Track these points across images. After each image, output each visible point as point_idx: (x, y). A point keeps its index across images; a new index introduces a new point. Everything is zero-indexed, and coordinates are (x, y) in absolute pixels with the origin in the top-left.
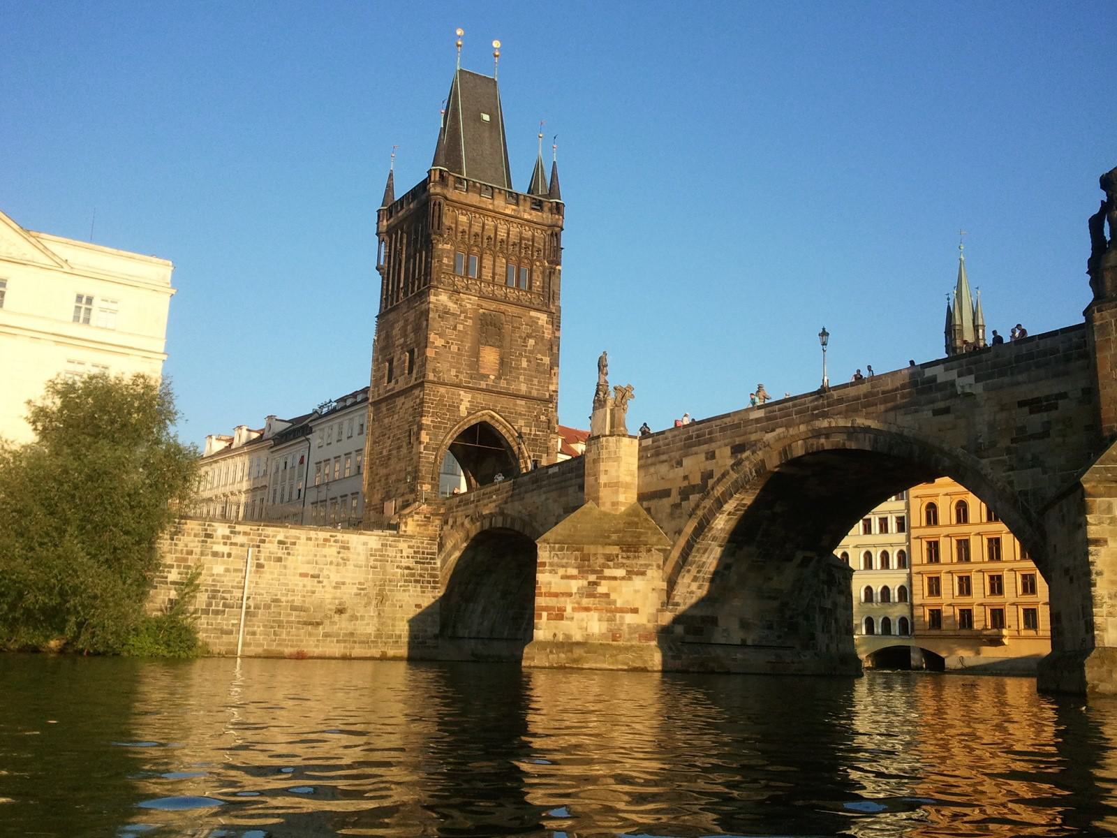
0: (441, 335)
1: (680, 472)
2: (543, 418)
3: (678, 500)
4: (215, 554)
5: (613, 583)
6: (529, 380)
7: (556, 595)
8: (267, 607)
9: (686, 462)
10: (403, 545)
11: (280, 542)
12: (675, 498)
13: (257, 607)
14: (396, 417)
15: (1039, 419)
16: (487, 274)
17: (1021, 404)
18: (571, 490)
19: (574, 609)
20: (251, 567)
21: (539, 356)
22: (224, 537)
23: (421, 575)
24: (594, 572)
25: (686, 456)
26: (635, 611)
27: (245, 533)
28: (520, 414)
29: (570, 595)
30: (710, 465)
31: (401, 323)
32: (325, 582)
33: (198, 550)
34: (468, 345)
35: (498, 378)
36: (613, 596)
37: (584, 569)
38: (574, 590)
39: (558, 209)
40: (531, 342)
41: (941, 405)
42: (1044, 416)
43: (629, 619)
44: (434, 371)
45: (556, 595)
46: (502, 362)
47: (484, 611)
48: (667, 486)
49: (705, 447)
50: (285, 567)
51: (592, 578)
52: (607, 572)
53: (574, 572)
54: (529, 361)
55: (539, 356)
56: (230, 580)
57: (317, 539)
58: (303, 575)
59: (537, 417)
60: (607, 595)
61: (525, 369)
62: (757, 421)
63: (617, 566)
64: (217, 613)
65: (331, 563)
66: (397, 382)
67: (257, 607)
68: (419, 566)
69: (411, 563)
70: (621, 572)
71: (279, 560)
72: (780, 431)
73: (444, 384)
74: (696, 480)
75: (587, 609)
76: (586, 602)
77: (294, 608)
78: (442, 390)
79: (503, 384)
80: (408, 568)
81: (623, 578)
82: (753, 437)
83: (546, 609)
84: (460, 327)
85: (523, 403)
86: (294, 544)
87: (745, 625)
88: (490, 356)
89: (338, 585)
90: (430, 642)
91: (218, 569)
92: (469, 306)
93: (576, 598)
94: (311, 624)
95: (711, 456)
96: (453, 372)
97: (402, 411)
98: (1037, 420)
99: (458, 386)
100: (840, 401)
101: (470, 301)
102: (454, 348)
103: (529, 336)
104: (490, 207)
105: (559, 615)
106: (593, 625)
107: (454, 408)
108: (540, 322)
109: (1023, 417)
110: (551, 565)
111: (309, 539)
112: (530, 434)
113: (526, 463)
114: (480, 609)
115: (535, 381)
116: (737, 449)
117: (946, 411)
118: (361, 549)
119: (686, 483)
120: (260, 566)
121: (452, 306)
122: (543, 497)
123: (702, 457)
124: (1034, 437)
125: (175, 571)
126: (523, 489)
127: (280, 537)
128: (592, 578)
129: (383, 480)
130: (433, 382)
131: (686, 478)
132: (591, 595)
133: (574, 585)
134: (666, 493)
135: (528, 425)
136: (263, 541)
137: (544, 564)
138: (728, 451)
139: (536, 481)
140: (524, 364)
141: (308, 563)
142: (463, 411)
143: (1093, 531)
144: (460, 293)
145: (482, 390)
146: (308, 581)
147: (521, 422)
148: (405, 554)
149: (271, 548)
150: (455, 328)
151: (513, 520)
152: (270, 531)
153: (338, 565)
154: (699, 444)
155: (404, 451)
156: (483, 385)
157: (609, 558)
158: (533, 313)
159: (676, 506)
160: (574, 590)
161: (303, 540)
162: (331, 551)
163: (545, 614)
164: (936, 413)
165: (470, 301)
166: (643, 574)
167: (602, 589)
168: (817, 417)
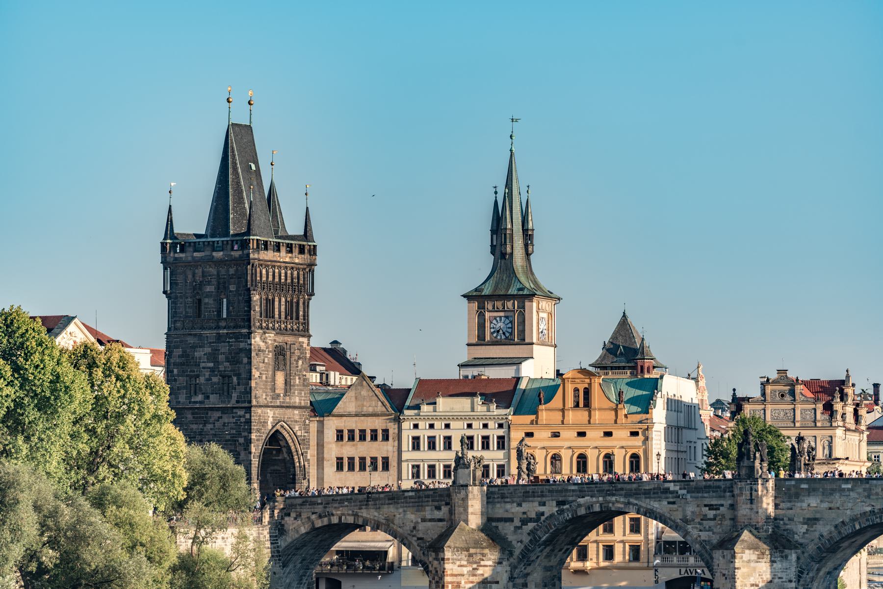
1: (521, 510)
3: (519, 524)
7: (456, 575)
9: (524, 504)
14: (209, 426)
15: (713, 512)
17: (706, 506)
21: (304, 373)
24: (476, 563)
25: (524, 501)
26: (497, 582)
28: (296, 421)
30: (542, 509)
31: (208, 350)
35: (285, 395)
38: (465, 573)
39: (313, 251)
40: (300, 362)
41: (671, 500)
42: (714, 512)
44: (256, 397)
45: (456, 575)
46: (287, 383)
47: (289, 573)
48: (510, 516)
51: (475, 566)
52: (482, 563)
53: (465, 563)
59: (304, 421)
62: (573, 491)
66: (208, 397)
72: (587, 498)
73: (261, 406)
74: (533, 515)
82: (571, 499)
83: (451, 583)
84: (266, 361)
88: (280, 377)
92: (270, 342)
93: (466, 577)
97: (218, 424)
98: (711, 514)
100: (622, 489)
102: (264, 376)
103: (299, 358)
109: (705, 510)
116: (560, 503)
117: (674, 503)
123: (536, 504)
124: (710, 519)
128: (475, 566)
130: (256, 406)
131: (524, 513)
133: (465, 570)
134: (511, 520)
137: (448, 559)
138: (554, 503)
139: (393, 499)
140: (297, 381)
143: (737, 565)
145: (278, 407)
154: (534, 497)
160: (465, 573)
163: (450, 586)
164: (669, 503)
168: (609, 495)
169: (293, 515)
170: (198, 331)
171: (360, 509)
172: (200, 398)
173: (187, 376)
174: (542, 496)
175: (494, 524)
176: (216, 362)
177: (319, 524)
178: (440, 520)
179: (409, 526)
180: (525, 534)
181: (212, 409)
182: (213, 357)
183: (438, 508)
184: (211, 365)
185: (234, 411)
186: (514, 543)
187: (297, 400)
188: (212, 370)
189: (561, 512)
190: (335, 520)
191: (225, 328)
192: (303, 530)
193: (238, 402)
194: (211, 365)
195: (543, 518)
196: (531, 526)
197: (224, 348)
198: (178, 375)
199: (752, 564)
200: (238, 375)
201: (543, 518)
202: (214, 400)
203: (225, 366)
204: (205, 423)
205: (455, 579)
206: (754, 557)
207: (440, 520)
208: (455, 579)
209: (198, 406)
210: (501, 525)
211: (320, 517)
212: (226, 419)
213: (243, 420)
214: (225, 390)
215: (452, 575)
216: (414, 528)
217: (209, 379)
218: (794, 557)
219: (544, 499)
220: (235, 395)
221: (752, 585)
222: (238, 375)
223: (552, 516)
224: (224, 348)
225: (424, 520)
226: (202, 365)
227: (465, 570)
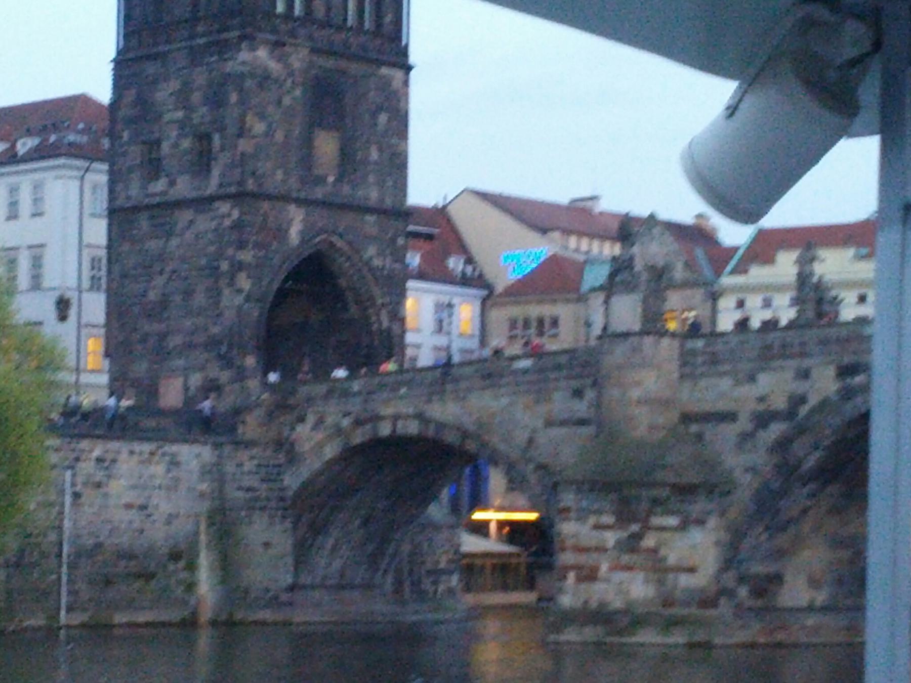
0: (262, 116)
5: (667, 535)
6: (381, 184)
10: (243, 455)
11: (99, 460)
12: (744, 423)
14: (174, 242)
18: (557, 396)
19: (612, 569)
20: (68, 499)
23: (268, 499)
24: (635, 520)
25: (763, 369)
26: (692, 570)
30: (800, 387)
31: (174, 85)
35: (339, 179)
36: (663, 552)
37: (624, 517)
40: (383, 118)
43: (685, 581)
47: (334, 549)
49: (793, 363)
50: (106, 495)
51: (635, 528)
52: (656, 521)
53: (608, 519)
54: (380, 150)
57: (141, 453)
58: (129, 506)
59: (393, 240)
60: (655, 551)
61: (376, 163)
63: (670, 513)
65: (160, 487)
66: (172, 183)
68: (265, 486)
69: (253, 481)
70: (672, 521)
71: (99, 485)
75: (629, 568)
76: (626, 559)
78: (266, 206)
79: (346, 189)
80: (249, 489)
81: (675, 529)
83: (572, 567)
84: (287, 101)
86: (114, 461)
87: (814, 583)
88: (327, 146)
89: (170, 519)
90: (284, 597)
94: (138, 576)
95: (804, 375)
96: (279, 175)
97: (189, 235)
99: (285, 198)
101: (299, 58)
102: (279, 136)
103: (380, 109)
106: (639, 588)
107: (281, 233)
110: (580, 510)
111: (132, 453)
112: (383, 268)
113: (378, 315)
114: (331, 542)
118: (194, 464)
119: (761, 407)
121: (274, 66)
122: (504, 401)
123: (789, 375)
126: (463, 385)
127: (97, 453)
128: (635, 528)
129: (152, 341)
130: (255, 196)
131: (761, 399)
132: (633, 550)
133: (611, 538)
134: (729, 417)
136: (77, 459)
137: (567, 510)
140: (374, 155)
141: (134, 487)
142: (294, 234)
144: (284, 45)
146: (133, 514)
148: (246, 469)
149: (87, 467)
150: (279, 102)
151: (441, 426)
152: (85, 444)
153: (169, 489)
155: (200, 299)
156: (319, 193)
157: (656, 502)
158: (384, 71)
159: (746, 437)
161: (124, 456)
162: (158, 469)
165: (299, 58)
166: (701, 522)
167: (649, 541)
169: (311, 419)
170: (161, 48)
171: (429, 401)
172: (160, 185)
173: (144, 143)
174: (803, 355)
175: (694, 428)
176: (188, 108)
177: (359, 437)
178: (582, 422)
179: (521, 437)
180: (762, 451)
181: (179, 204)
182: (183, 98)
183: (578, 393)
184: (180, 114)
185: (217, 204)
186: (737, 473)
188: (182, 125)
190: (385, 430)
191: (203, 36)
192: (330, 451)
193: (221, 185)
194: (180, 114)
195: (804, 410)
196: (776, 430)
197: (200, 77)
198: (128, 143)
200: (222, 130)
201: (804, 410)
202: (184, 187)
203: (202, 114)
204: (169, 235)
205: (582, 559)
207: (582, 422)
208: (582, 559)
209: (158, 199)
210: (710, 431)
211: (358, 423)
212: (204, 223)
213: (227, 222)
214: (202, 161)
216: (531, 441)
217: (176, 145)
219: (807, 363)
220: (216, 172)
222: (222, 130)
223: (824, 404)
224: (200, 77)
225: (549, 423)
226: (167, 117)
227: (611, 538)
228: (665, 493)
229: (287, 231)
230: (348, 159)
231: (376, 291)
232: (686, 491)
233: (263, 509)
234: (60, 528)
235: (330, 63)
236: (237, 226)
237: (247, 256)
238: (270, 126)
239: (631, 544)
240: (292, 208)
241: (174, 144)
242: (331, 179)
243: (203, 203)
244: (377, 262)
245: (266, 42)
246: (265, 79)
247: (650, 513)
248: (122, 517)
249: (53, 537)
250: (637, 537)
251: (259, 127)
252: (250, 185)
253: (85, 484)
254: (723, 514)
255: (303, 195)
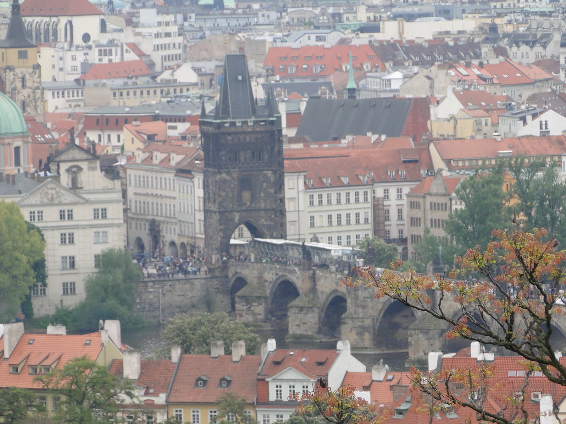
0: (224, 191)
2: (273, 216)
4: (150, 292)
8: (169, 307)
10: (214, 280)
13: (165, 308)
16: (242, 159)
22: (152, 286)
26: (260, 315)
27: (158, 284)
29: (243, 310)
32: (187, 297)
33: (144, 291)
34: (236, 193)
35: (251, 203)
40: (265, 184)
43: (259, 317)
44: (223, 207)
45: (241, 310)
51: (249, 306)
52: (253, 304)
53: (244, 304)
55: (269, 190)
56: (155, 300)
58: (179, 295)
59: (270, 217)
60: (253, 310)
63: (255, 302)
64: (152, 311)
67: (165, 308)
69: (218, 286)
70: (256, 304)
71: (170, 291)
73: (226, 212)
75: (248, 314)
76: (248, 312)
77: (178, 307)
78: (227, 214)
79: (253, 205)
80: (217, 288)
81: (257, 306)
83: (239, 314)
84: (232, 186)
85: (263, 212)
88: (246, 195)
89: (191, 298)
91: (151, 297)
96: (231, 205)
99: (234, 211)
103: (264, 182)
104: (241, 130)
105: (241, 316)
108: (268, 175)
115: (268, 201)
116: (276, 274)
118: (198, 284)
120: (164, 294)
121: (228, 178)
125: (138, 299)
128: (249, 306)
132: (249, 310)
133: (245, 308)
135: (266, 221)
140: (262, 195)
146: (181, 297)
147: (263, 220)
149: (167, 287)
150: (230, 187)
152: (166, 282)
156: (244, 208)
158: (264, 172)
166: (261, 304)
167: (252, 309)
187: (263, 205)
189: (277, 279)
192: (234, 279)
199: (296, 315)
205: (240, 312)
206: (297, 311)
215: (239, 310)
218: (317, 310)
221: (297, 325)
227: (245, 308)
228: (254, 298)
229: (234, 220)
230: (253, 198)
231: (265, 231)
232: (259, 298)
233: (221, 293)
234: (159, 302)
235: (246, 173)
236: (220, 220)
237: (222, 227)
238: (227, 193)
239: (249, 309)
240: (235, 213)
241: (212, 195)
242: (248, 203)
243: (215, 212)
244: (265, 223)
245: (224, 172)
246: (224, 181)
247: (252, 302)
248: (177, 298)
249: (158, 304)
250: (250, 307)
251: (224, 194)
252: (222, 209)
253: (167, 291)
254: (266, 302)
255: (239, 209)
